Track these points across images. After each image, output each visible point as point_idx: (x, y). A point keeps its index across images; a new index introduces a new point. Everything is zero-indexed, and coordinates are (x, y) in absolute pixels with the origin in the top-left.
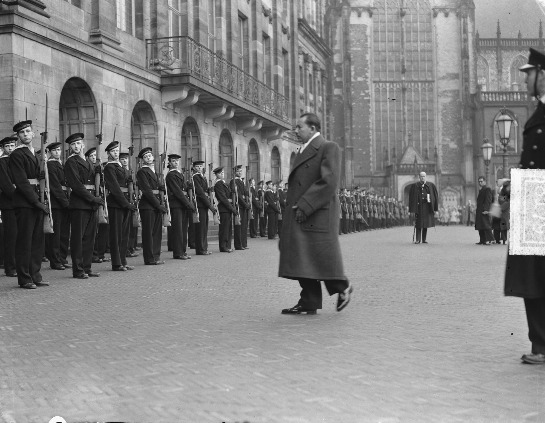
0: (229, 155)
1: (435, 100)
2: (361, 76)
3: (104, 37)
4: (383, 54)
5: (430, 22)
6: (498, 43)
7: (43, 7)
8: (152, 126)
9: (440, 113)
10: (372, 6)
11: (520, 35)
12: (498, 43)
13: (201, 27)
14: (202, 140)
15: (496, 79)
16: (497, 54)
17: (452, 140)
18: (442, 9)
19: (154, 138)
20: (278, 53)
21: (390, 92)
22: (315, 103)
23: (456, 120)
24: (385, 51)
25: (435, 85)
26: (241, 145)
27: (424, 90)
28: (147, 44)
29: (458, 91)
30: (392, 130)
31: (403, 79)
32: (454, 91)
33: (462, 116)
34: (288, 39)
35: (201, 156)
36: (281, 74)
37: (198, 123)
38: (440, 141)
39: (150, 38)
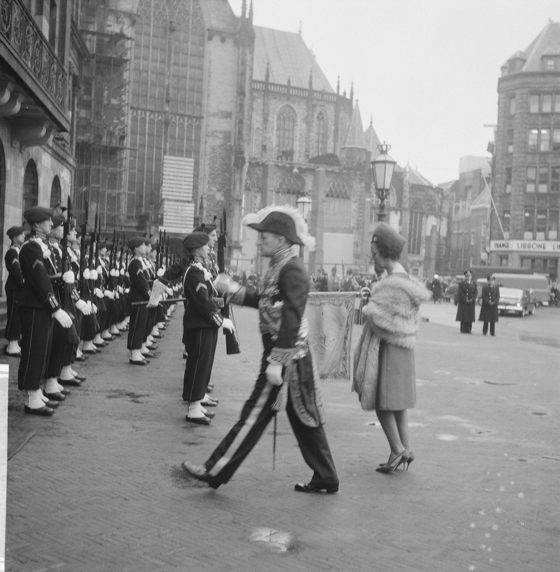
1: (203, 140)
2: (115, 98)
4: (145, 75)
5: (203, 45)
6: (266, 87)
9: (208, 157)
10: (135, 11)
11: (289, 82)
12: (266, 87)
15: (261, 128)
16: (264, 99)
17: (219, 190)
18: (219, 32)
21: (149, 123)
23: (225, 167)
24: (147, 72)
25: (204, 122)
27: (190, 126)
29: (230, 132)
30: (150, 171)
31: (167, 109)
32: (225, 132)
33: (232, 164)
38: (206, 190)
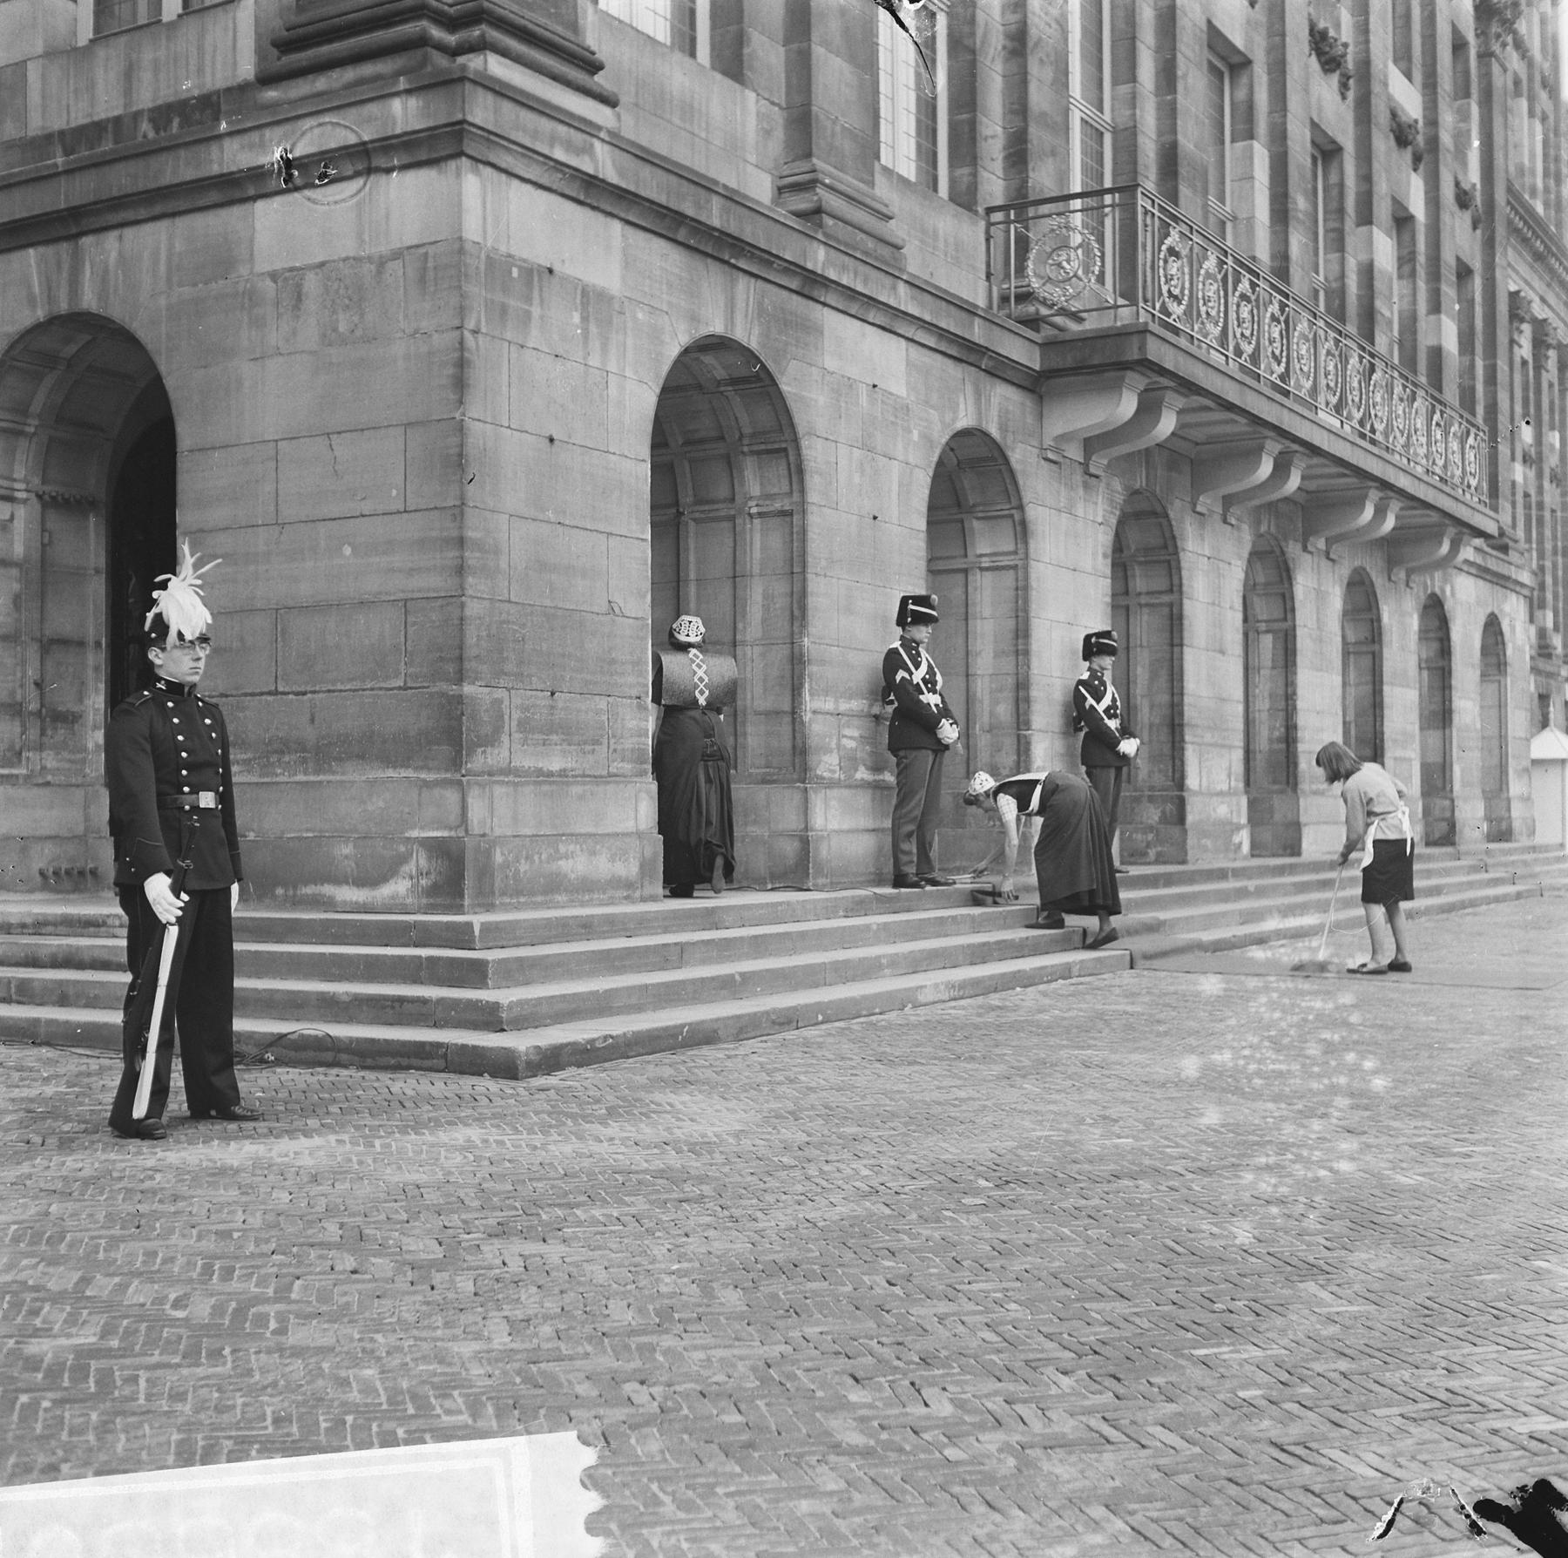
0: (1276, 626)
3: (831, 188)
7: (594, 67)
8: (1007, 524)
13: (1183, 171)
14: (1184, 573)
19: (1015, 567)
20: (1443, 271)
22: (1540, 454)
26: (1318, 591)
28: (990, 225)
34: (1475, 228)
35: (1181, 631)
36: (1450, 341)
37: (1172, 515)
39: (999, 202)
